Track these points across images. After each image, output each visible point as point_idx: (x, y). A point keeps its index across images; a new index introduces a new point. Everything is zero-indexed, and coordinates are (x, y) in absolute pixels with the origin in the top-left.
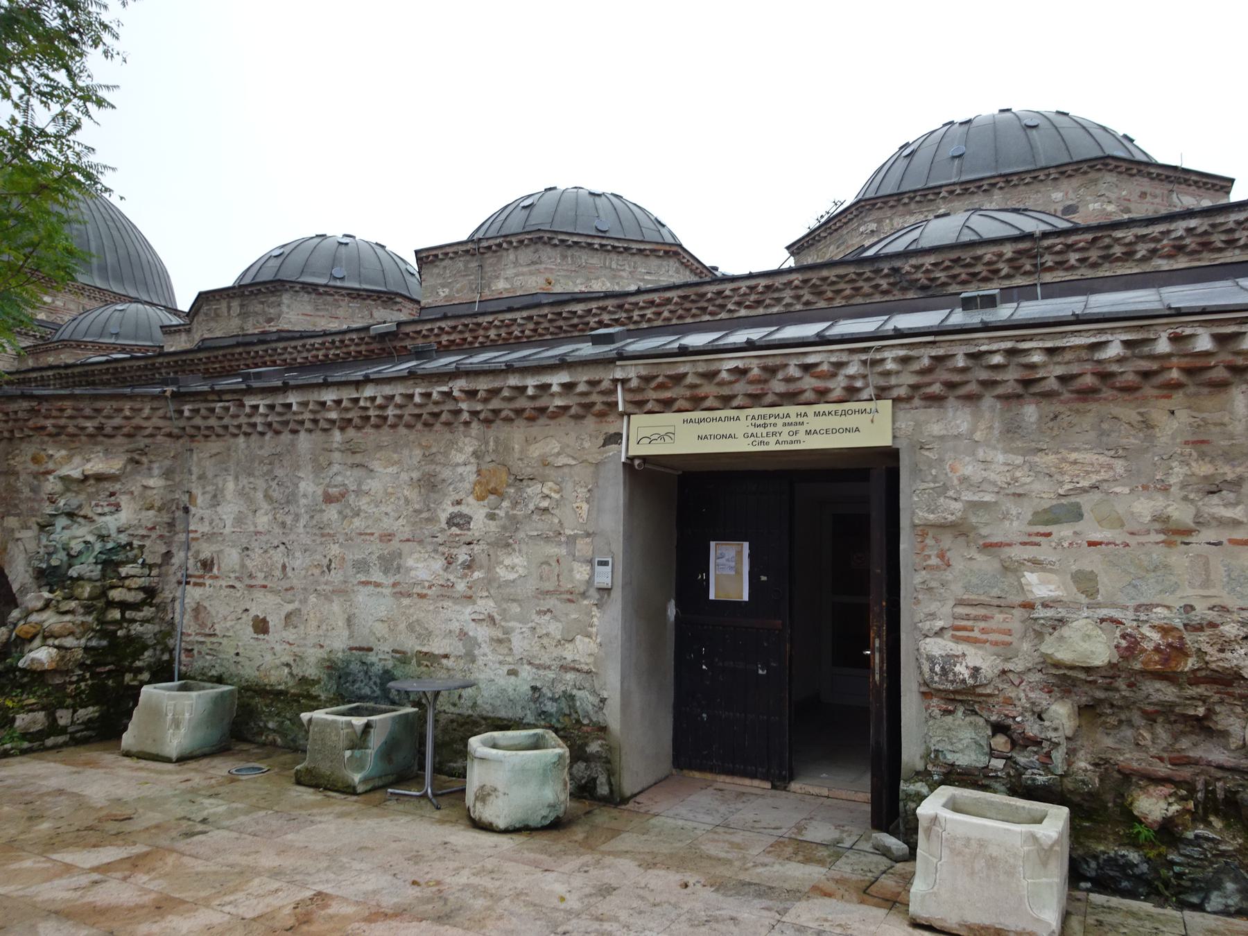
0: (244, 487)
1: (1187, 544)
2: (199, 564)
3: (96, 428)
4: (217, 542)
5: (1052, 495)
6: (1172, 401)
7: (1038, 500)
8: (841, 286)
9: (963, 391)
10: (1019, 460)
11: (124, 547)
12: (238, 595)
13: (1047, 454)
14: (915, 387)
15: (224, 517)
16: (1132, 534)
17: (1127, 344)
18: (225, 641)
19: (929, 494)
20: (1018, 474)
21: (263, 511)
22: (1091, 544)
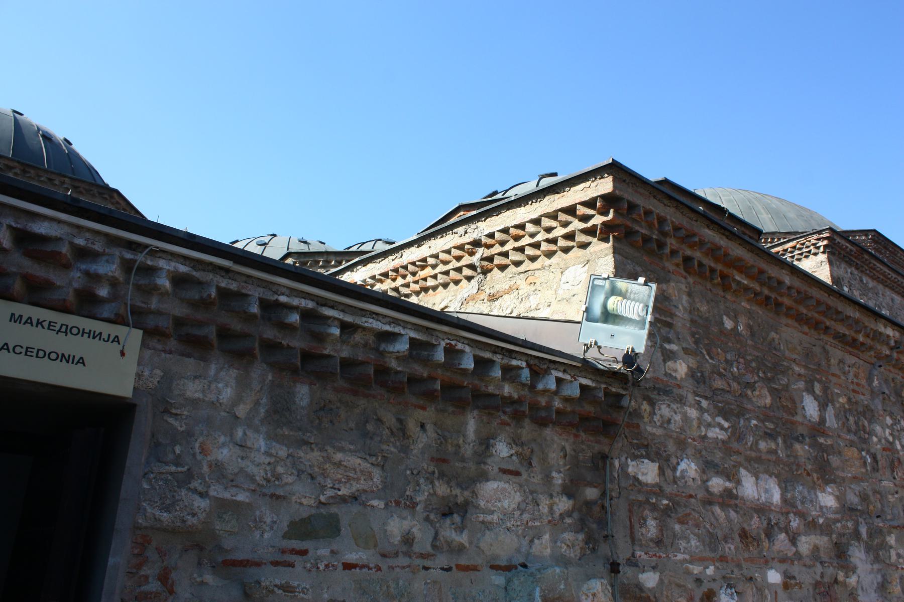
1: (426, 568)
5: (312, 502)
6: (426, 413)
7: (297, 506)
10: (283, 452)
13: (312, 450)
14: (179, 322)
16: (384, 556)
19: (166, 480)
20: (280, 470)
22: (348, 566)
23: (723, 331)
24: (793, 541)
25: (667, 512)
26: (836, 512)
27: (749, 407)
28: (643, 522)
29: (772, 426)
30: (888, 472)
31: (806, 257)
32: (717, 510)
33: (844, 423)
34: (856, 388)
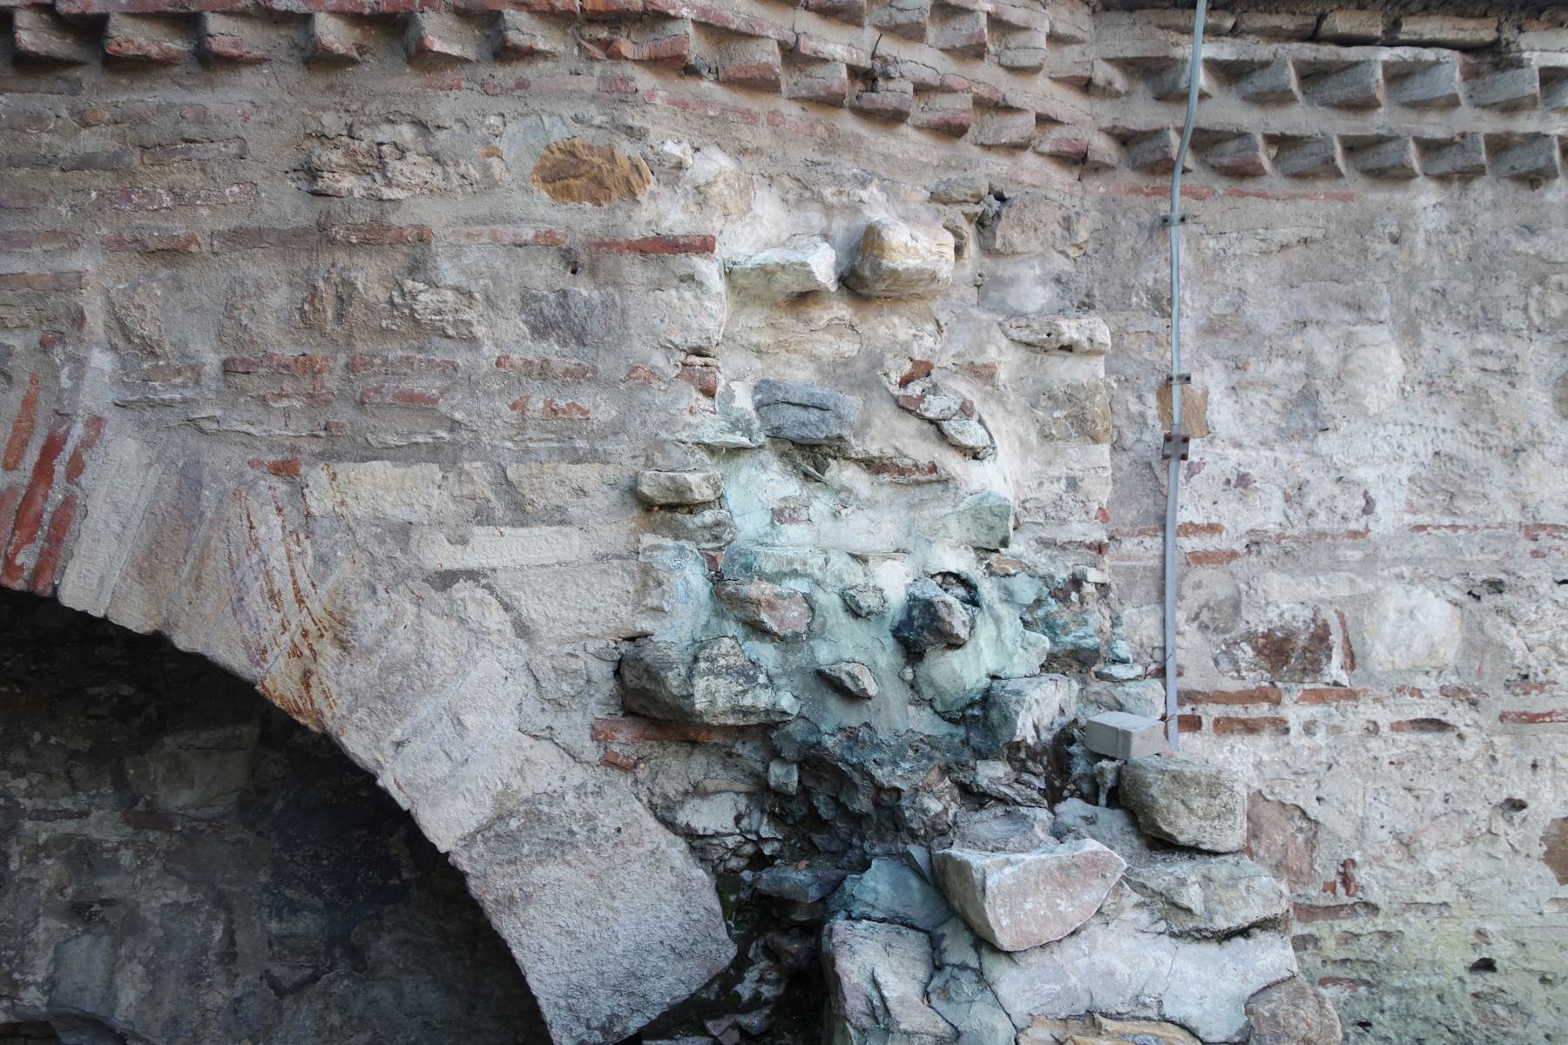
0: (1454, 364)
2: (1246, 652)
3: (855, 72)
4: (1336, 565)
11: (1061, 595)
12: (1467, 752)
15: (1362, 473)
18: (1411, 928)
21: (1550, 453)
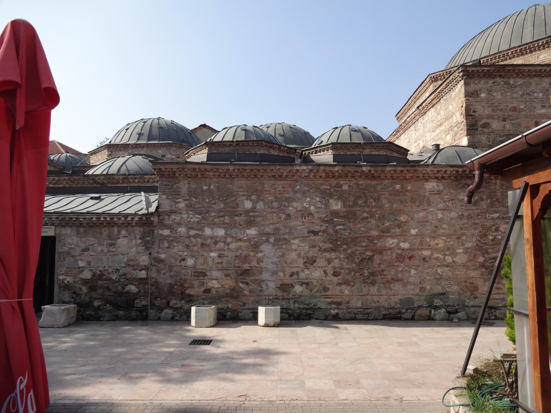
8: (80, 181)
9: (69, 225)
10: (79, 239)
14: (60, 223)
17: (96, 218)
22: (91, 255)
23: (203, 191)
24: (228, 245)
25: (172, 241)
26: (256, 235)
27: (212, 210)
28: (163, 243)
29: (223, 214)
30: (300, 219)
31: (458, 83)
32: (192, 239)
33: (269, 206)
34: (282, 192)
